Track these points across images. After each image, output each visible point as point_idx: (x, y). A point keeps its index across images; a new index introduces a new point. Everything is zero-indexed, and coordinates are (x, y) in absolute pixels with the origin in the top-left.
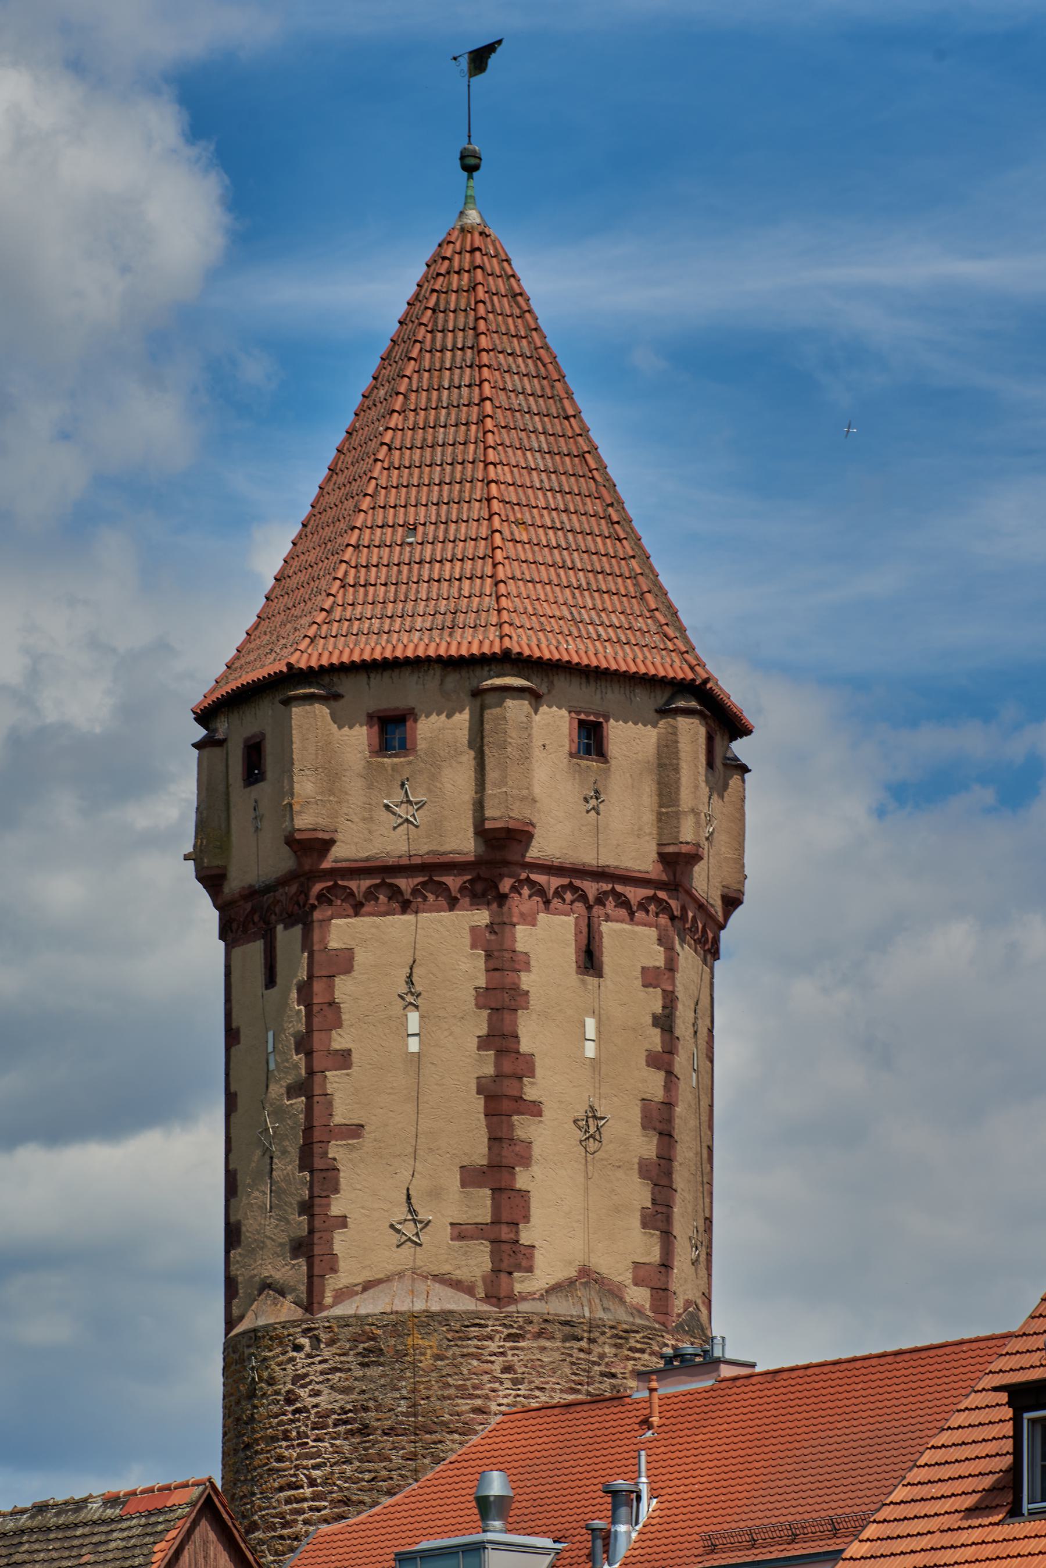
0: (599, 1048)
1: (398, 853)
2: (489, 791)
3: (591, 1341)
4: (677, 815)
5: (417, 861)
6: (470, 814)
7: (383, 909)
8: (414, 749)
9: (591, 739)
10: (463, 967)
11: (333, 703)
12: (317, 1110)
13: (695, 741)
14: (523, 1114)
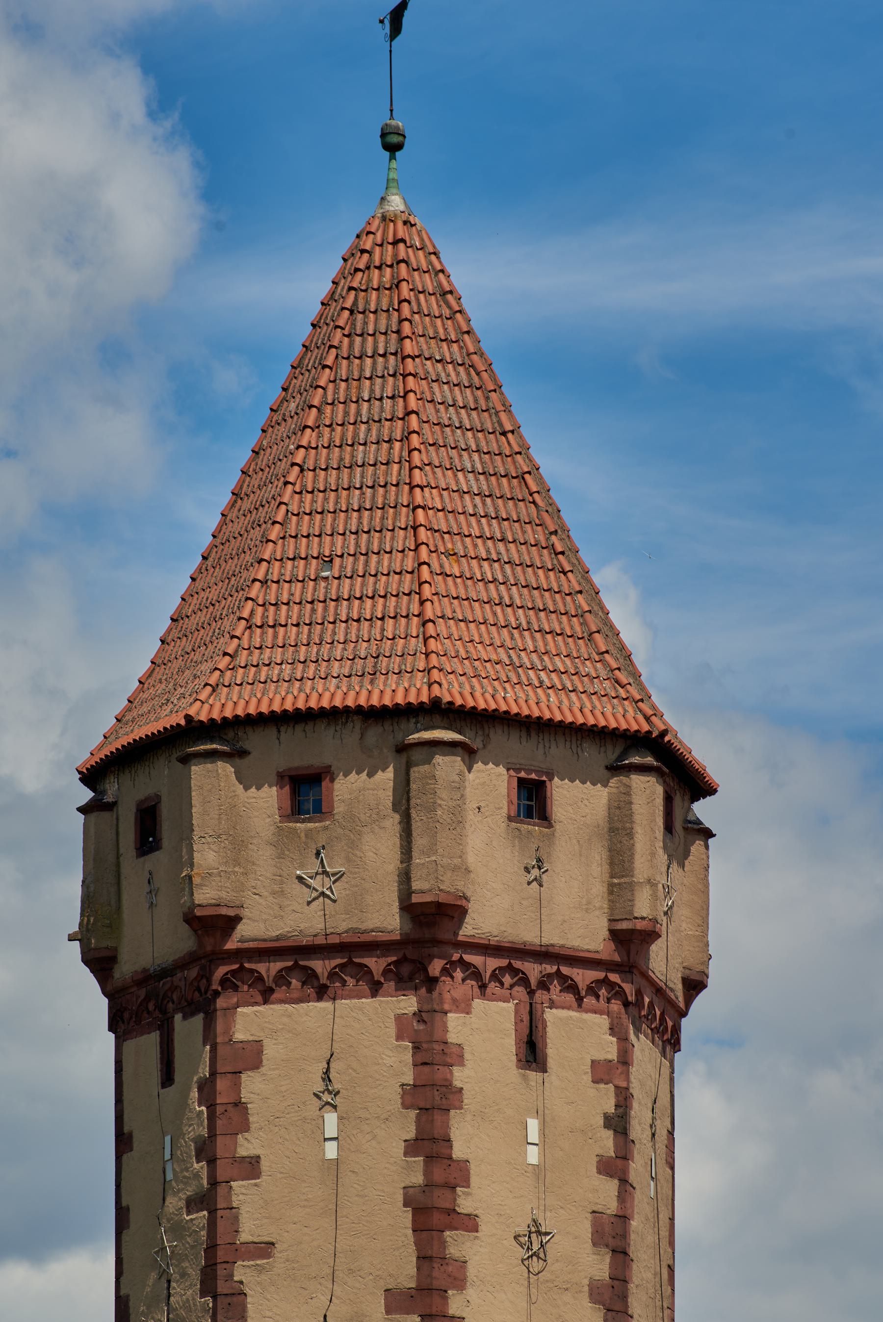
0: (543, 1154)
1: (314, 932)
2: (416, 860)
4: (631, 887)
5: (336, 940)
6: (395, 887)
7: (295, 995)
8: (331, 813)
9: (532, 801)
10: (389, 1061)
11: (238, 761)
12: (221, 1226)
13: (651, 802)
14: (456, 1229)
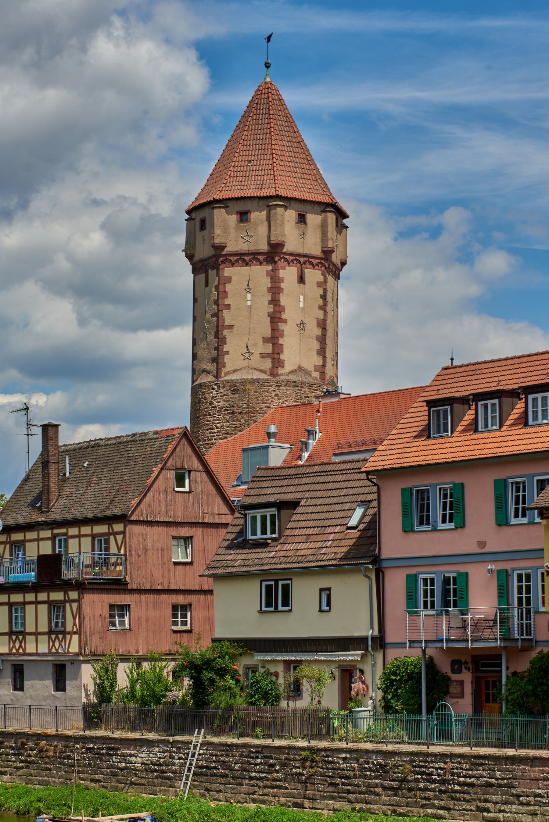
3: (302, 387)
